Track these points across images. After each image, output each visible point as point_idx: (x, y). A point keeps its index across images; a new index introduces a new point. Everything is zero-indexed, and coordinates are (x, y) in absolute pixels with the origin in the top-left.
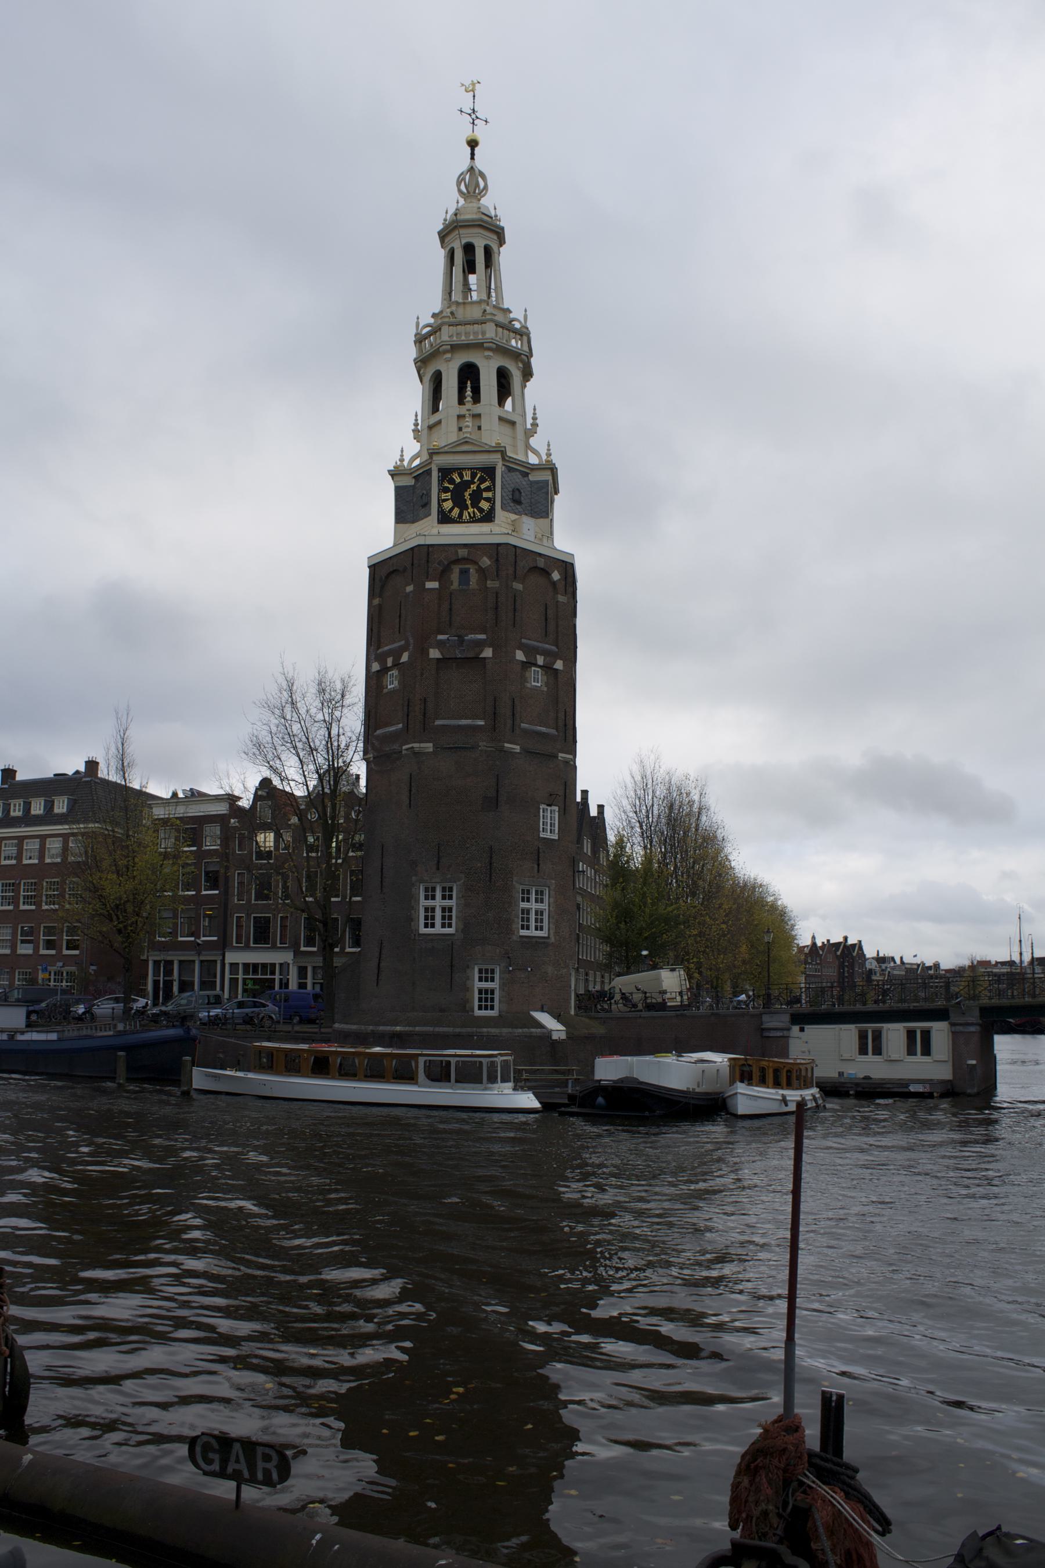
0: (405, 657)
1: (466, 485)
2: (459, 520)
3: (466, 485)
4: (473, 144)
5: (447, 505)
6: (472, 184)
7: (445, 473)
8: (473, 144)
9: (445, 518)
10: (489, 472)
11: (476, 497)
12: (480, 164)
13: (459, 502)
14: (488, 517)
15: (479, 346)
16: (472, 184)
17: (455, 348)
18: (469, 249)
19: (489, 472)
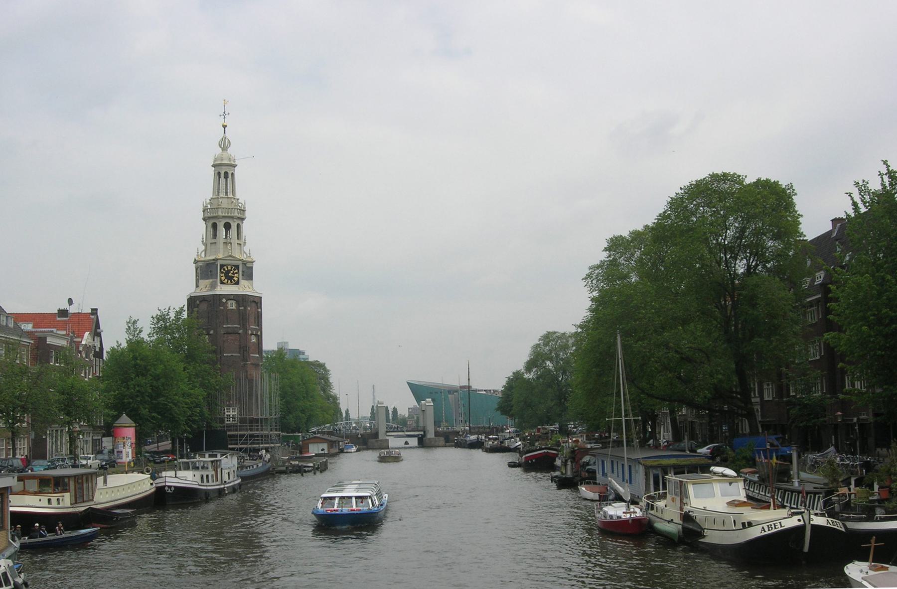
0: (212, 332)
1: (229, 271)
3: (229, 271)
5: (223, 278)
6: (224, 145)
7: (222, 266)
8: (225, 127)
9: (222, 283)
10: (237, 267)
12: (228, 135)
14: (237, 283)
15: (232, 217)
16: (224, 145)
17: (224, 217)
18: (226, 174)
19: (237, 267)
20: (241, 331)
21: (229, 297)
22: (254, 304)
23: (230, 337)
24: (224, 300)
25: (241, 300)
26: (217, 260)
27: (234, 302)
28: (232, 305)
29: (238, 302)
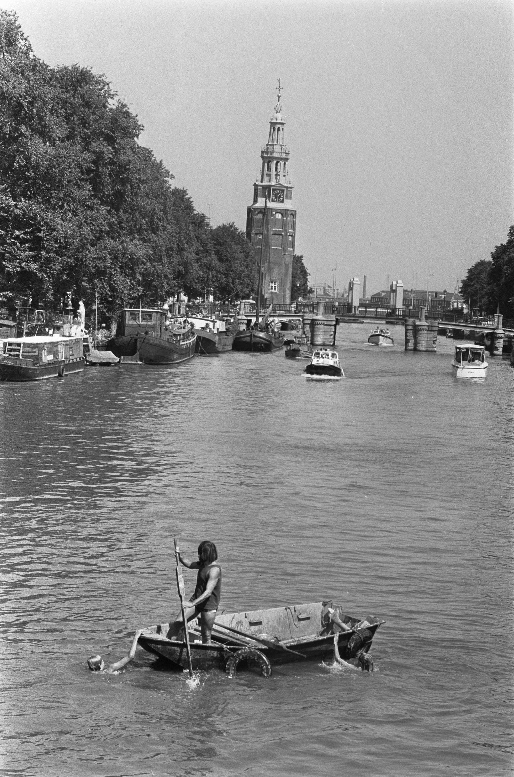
2: (276, 201)
3: (278, 194)
4: (279, 97)
7: (274, 190)
8: (279, 97)
9: (273, 201)
11: (280, 197)
13: (276, 197)
14: (282, 201)
18: (279, 129)
20: (283, 233)
21: (278, 211)
22: (292, 216)
23: (277, 237)
24: (274, 213)
25: (284, 212)
26: (271, 186)
27: (280, 215)
28: (279, 216)
29: (282, 214)
